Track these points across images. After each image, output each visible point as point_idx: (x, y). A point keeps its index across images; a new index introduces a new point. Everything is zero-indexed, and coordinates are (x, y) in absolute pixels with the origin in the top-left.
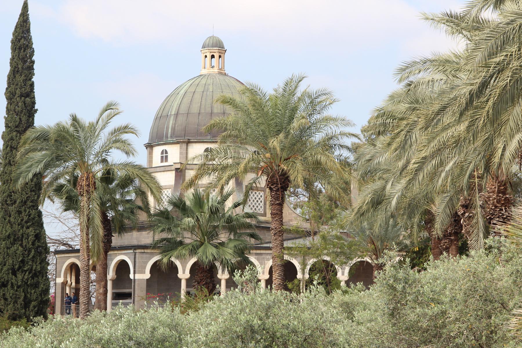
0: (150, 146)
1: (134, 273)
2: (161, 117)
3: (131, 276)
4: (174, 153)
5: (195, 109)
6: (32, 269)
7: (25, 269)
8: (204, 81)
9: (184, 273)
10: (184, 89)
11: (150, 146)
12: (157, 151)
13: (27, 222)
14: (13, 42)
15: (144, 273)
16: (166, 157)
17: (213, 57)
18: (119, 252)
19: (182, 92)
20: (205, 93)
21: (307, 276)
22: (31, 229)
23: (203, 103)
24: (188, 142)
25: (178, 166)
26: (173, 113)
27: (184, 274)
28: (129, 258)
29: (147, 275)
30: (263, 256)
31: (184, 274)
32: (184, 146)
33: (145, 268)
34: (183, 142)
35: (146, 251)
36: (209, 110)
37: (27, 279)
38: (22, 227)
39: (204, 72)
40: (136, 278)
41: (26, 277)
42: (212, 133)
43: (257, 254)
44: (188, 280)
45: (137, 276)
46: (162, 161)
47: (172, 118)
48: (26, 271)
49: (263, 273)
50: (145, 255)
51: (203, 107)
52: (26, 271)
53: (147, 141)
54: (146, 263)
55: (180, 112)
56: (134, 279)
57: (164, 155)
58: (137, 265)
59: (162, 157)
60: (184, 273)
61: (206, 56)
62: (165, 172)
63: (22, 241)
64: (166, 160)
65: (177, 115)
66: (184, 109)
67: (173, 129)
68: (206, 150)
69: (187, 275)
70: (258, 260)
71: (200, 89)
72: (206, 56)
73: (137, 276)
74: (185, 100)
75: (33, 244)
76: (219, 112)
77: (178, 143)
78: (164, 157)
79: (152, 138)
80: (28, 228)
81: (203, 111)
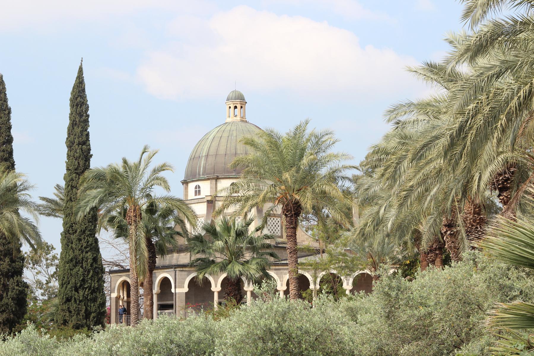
0: (185, 183)
1: (175, 288)
2: (194, 159)
3: (173, 290)
4: (206, 188)
5: (222, 151)
6: (91, 287)
7: (86, 286)
8: (228, 128)
9: (216, 286)
10: (212, 135)
11: (185, 183)
12: (192, 186)
13: (85, 248)
14: (71, 100)
15: (184, 287)
16: (199, 191)
17: (236, 107)
19: (211, 137)
20: (230, 137)
21: (318, 287)
22: (89, 253)
23: (228, 146)
24: (217, 179)
25: (209, 198)
26: (204, 155)
27: (216, 287)
28: (171, 275)
29: (186, 289)
30: (281, 271)
31: (216, 287)
32: (214, 181)
34: (213, 179)
35: (184, 269)
36: (233, 151)
37: (87, 295)
38: (82, 252)
39: (229, 120)
40: (177, 292)
41: (86, 293)
42: (237, 169)
43: (276, 269)
44: (219, 293)
45: (178, 290)
46: (196, 195)
47: (203, 158)
48: (86, 288)
49: (282, 285)
50: (183, 273)
51: (228, 149)
52: (86, 288)
53: (183, 179)
54: (185, 279)
55: (210, 154)
56: (175, 293)
58: (177, 281)
59: (196, 191)
60: (216, 286)
61: (230, 107)
62: (199, 204)
63: (82, 263)
64: (199, 194)
65: (207, 156)
66: (212, 151)
67: (205, 168)
68: (232, 184)
69: (219, 288)
71: (226, 135)
72: (230, 107)
73: (178, 290)
74: (213, 143)
75: (91, 265)
76: (242, 152)
77: (208, 179)
78: (198, 191)
79: (187, 175)
80: (87, 252)
81: (228, 152)
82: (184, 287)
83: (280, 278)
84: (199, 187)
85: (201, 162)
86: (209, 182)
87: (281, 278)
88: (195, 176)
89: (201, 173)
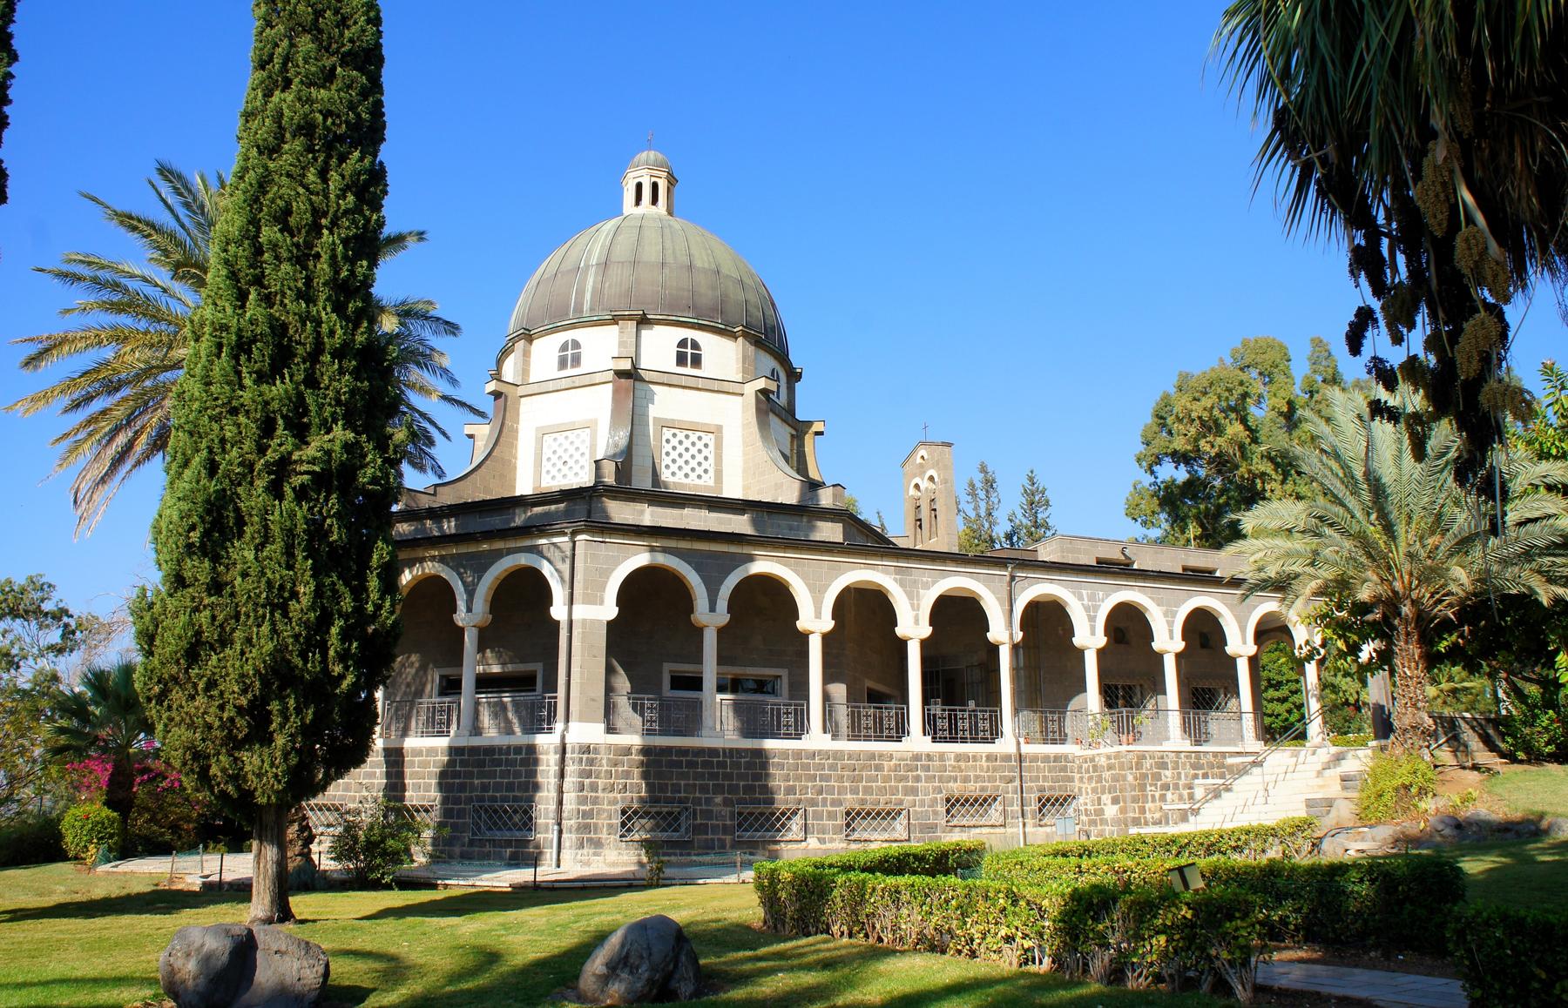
3: (558, 611)
4: (602, 347)
5: (651, 253)
15: (602, 603)
18: (512, 544)
23: (668, 244)
24: (643, 321)
29: (610, 611)
33: (603, 588)
34: (630, 318)
43: (899, 570)
44: (722, 632)
47: (592, 271)
51: (669, 252)
54: (606, 574)
57: (570, 352)
60: (712, 609)
65: (605, 265)
66: (622, 251)
67: (598, 293)
68: (683, 343)
69: (722, 617)
70: (902, 584)
74: (620, 238)
77: (615, 320)
82: (602, 603)
83: (910, 596)
84: (576, 345)
85: (584, 281)
86: (614, 330)
87: (912, 596)
88: (565, 315)
89: (586, 307)
